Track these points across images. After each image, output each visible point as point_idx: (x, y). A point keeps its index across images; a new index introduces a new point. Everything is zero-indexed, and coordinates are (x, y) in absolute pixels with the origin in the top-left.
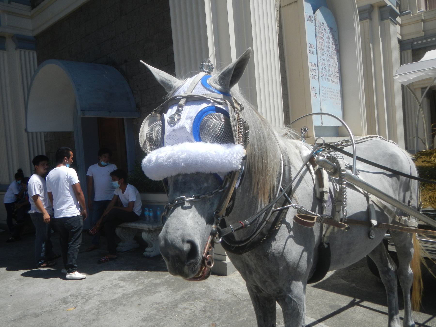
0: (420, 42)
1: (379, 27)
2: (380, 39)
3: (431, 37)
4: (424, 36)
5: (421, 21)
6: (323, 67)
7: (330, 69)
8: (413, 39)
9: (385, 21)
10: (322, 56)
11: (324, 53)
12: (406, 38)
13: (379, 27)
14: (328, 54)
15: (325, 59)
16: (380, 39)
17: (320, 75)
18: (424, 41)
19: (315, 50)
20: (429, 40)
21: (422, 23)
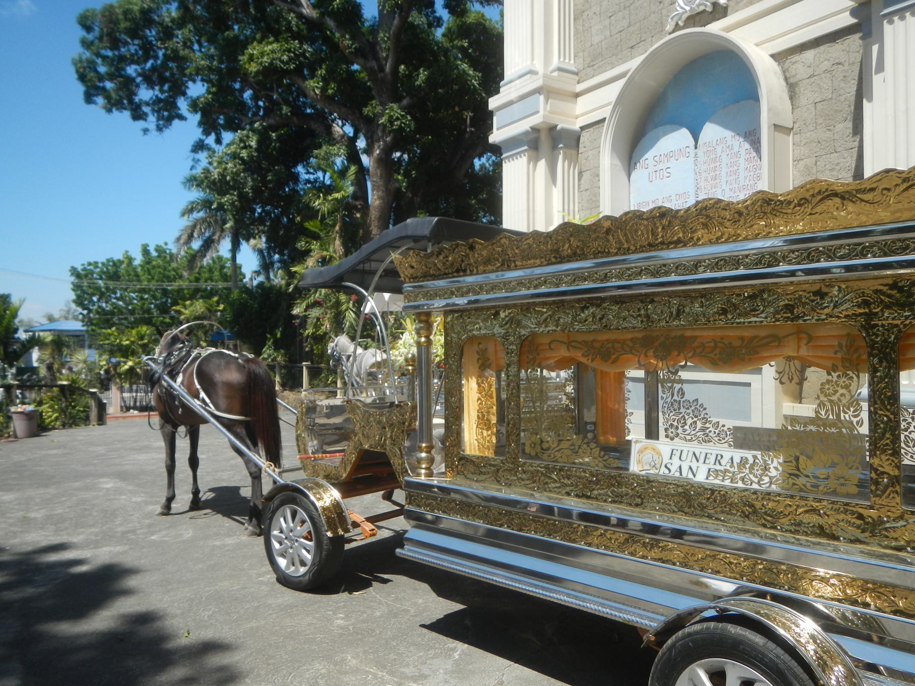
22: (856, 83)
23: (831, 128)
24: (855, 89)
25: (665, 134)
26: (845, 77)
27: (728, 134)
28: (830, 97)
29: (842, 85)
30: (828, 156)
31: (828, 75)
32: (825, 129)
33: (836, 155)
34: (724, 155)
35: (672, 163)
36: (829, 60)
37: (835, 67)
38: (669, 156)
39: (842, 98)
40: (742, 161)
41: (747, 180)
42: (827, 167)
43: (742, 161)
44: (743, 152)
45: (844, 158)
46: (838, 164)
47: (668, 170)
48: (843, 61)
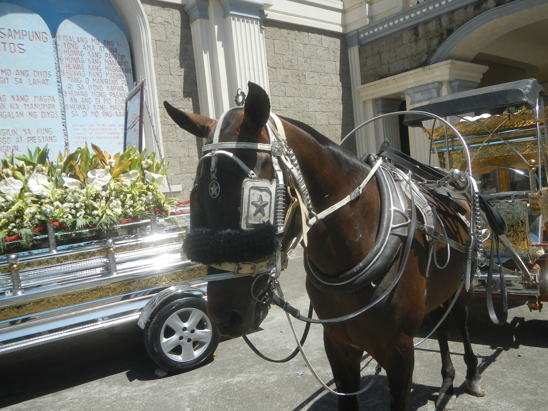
0: (366, 34)
1: (216, 27)
2: (219, 44)
3: (377, 26)
4: (369, 25)
5: (365, 2)
6: (79, 98)
7: (102, 99)
8: (357, 30)
9: (227, 18)
10: (75, 85)
11: (83, 79)
12: (351, 29)
13: (216, 27)
14: (97, 78)
15: (86, 86)
16: (219, 44)
17: (68, 112)
18: (371, 32)
19: (54, 79)
20: (376, 30)
21: (367, 5)
22: (180, 39)
23: (168, 59)
24: (179, 42)
25: (13, 11)
26: (173, 32)
27: (89, 37)
28: (165, 40)
29: (172, 36)
30: (167, 76)
31: (162, 26)
32: (163, 59)
33: (171, 76)
34: (85, 52)
35: (25, 41)
36: (161, 17)
37: (166, 23)
38: (22, 34)
39: (173, 44)
40: (102, 60)
41: (108, 76)
42: (167, 82)
43: (102, 60)
44: (103, 55)
45: (177, 80)
46: (173, 82)
47: (20, 46)
48: (170, 21)
